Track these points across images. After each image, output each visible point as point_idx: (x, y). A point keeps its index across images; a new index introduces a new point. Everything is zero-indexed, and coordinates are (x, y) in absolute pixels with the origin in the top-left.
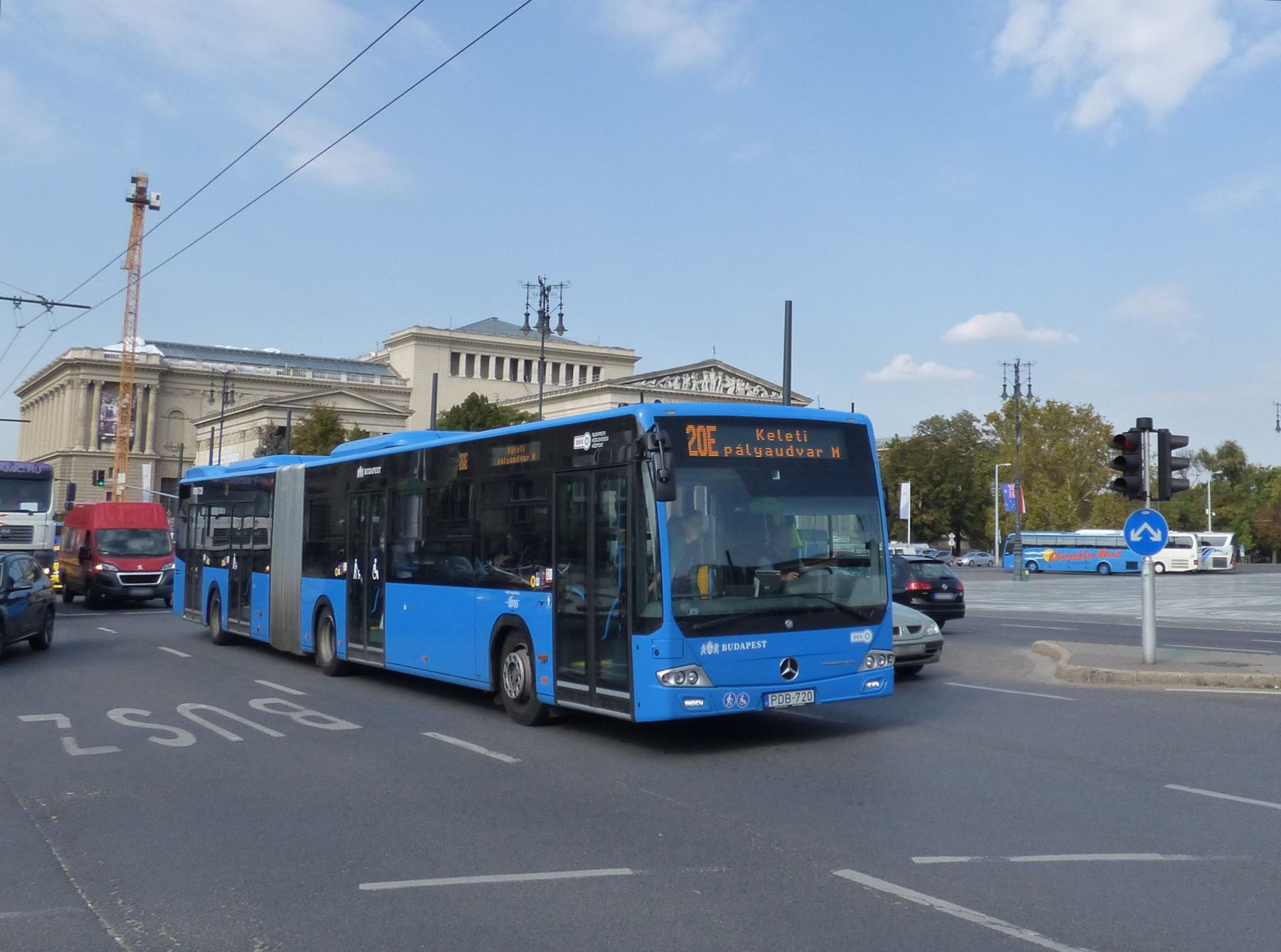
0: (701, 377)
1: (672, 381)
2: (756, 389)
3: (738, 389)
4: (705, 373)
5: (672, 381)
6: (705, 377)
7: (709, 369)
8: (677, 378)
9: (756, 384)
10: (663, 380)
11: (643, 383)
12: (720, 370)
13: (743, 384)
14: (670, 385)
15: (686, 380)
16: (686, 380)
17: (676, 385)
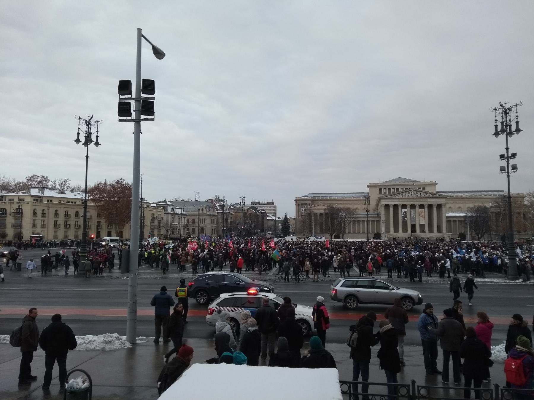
0: (409, 193)
1: (400, 195)
2: (428, 194)
3: (421, 195)
4: (410, 192)
5: (400, 195)
6: (410, 193)
7: (411, 190)
8: (401, 194)
9: (428, 193)
10: (397, 195)
11: (390, 196)
12: (415, 190)
13: (423, 193)
14: (399, 196)
15: (404, 194)
16: (404, 194)
17: (401, 196)
